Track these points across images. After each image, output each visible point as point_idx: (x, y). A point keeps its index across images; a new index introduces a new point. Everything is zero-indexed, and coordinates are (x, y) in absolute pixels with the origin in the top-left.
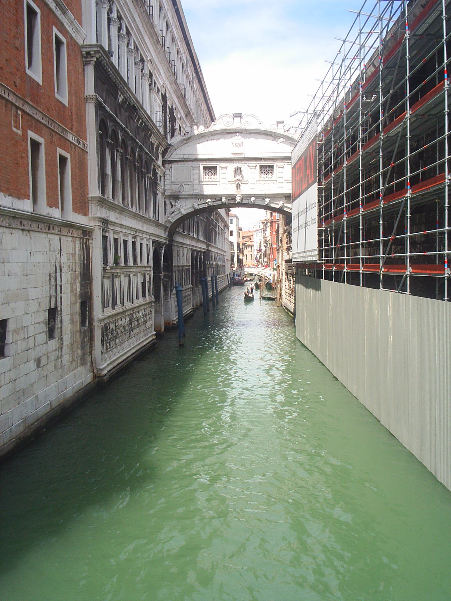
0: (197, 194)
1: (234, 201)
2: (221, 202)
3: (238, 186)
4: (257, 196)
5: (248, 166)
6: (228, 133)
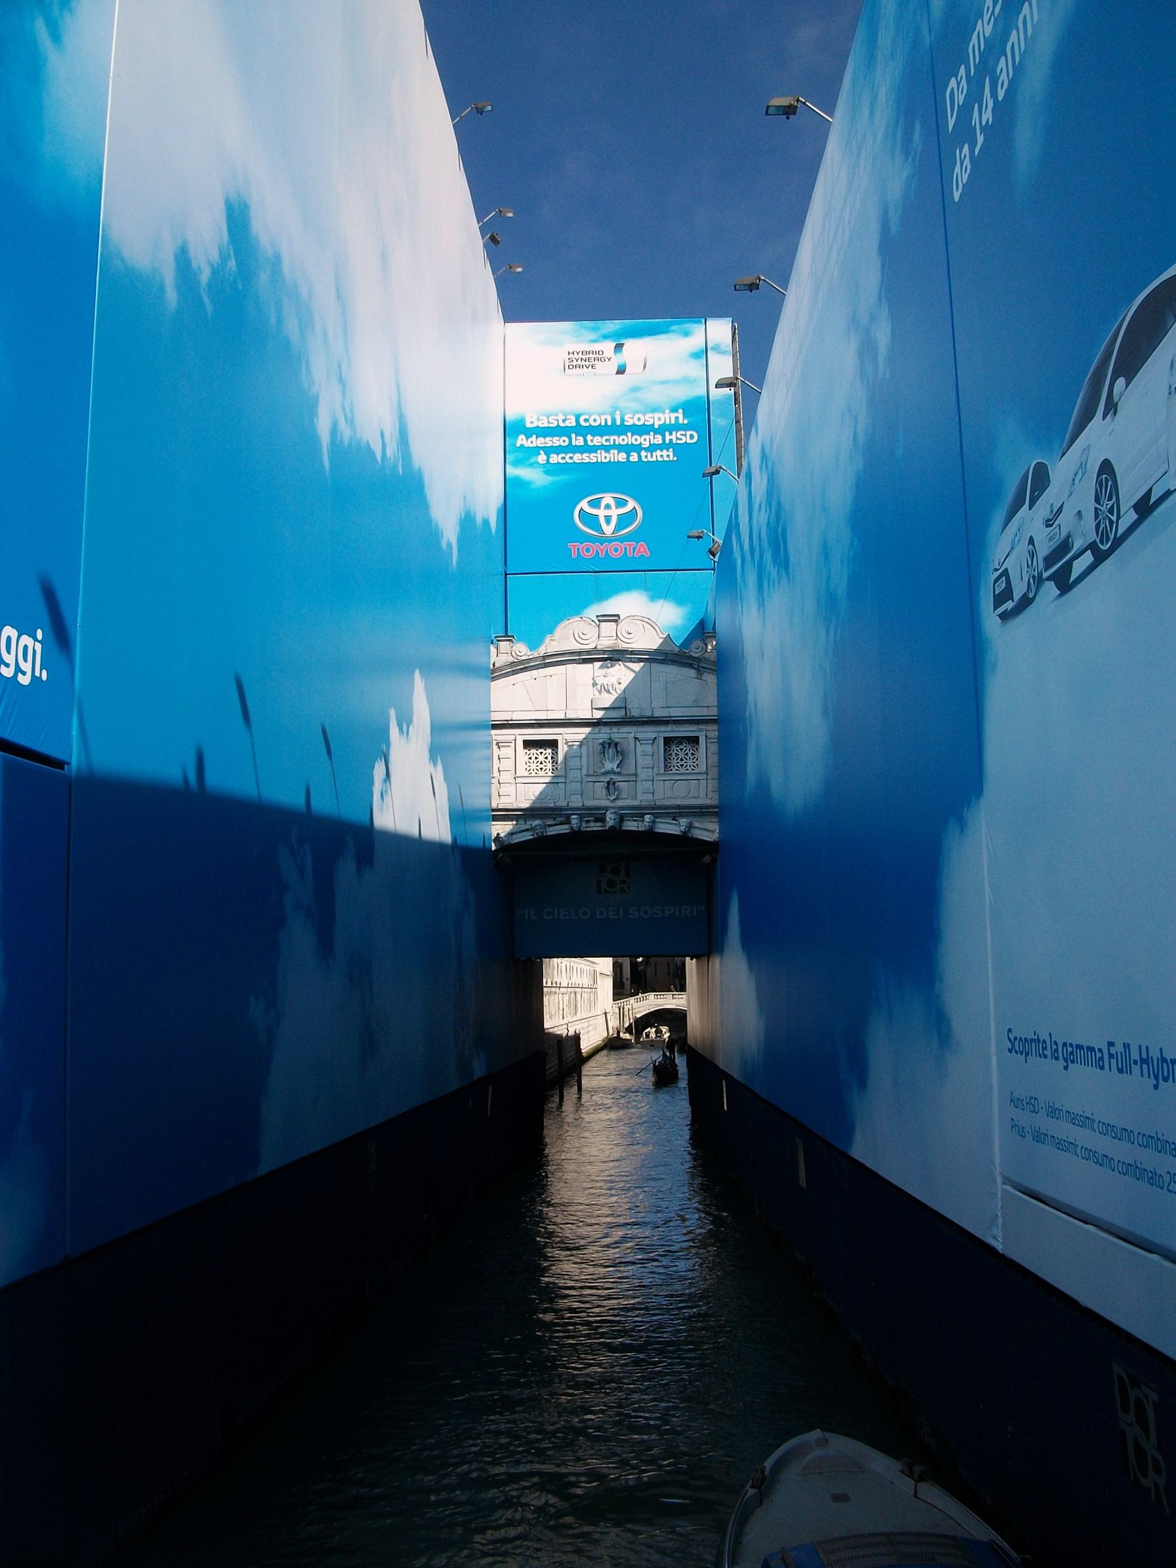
2: (567, 826)
3: (610, 785)
4: (660, 811)
5: (636, 738)
6: (585, 661)
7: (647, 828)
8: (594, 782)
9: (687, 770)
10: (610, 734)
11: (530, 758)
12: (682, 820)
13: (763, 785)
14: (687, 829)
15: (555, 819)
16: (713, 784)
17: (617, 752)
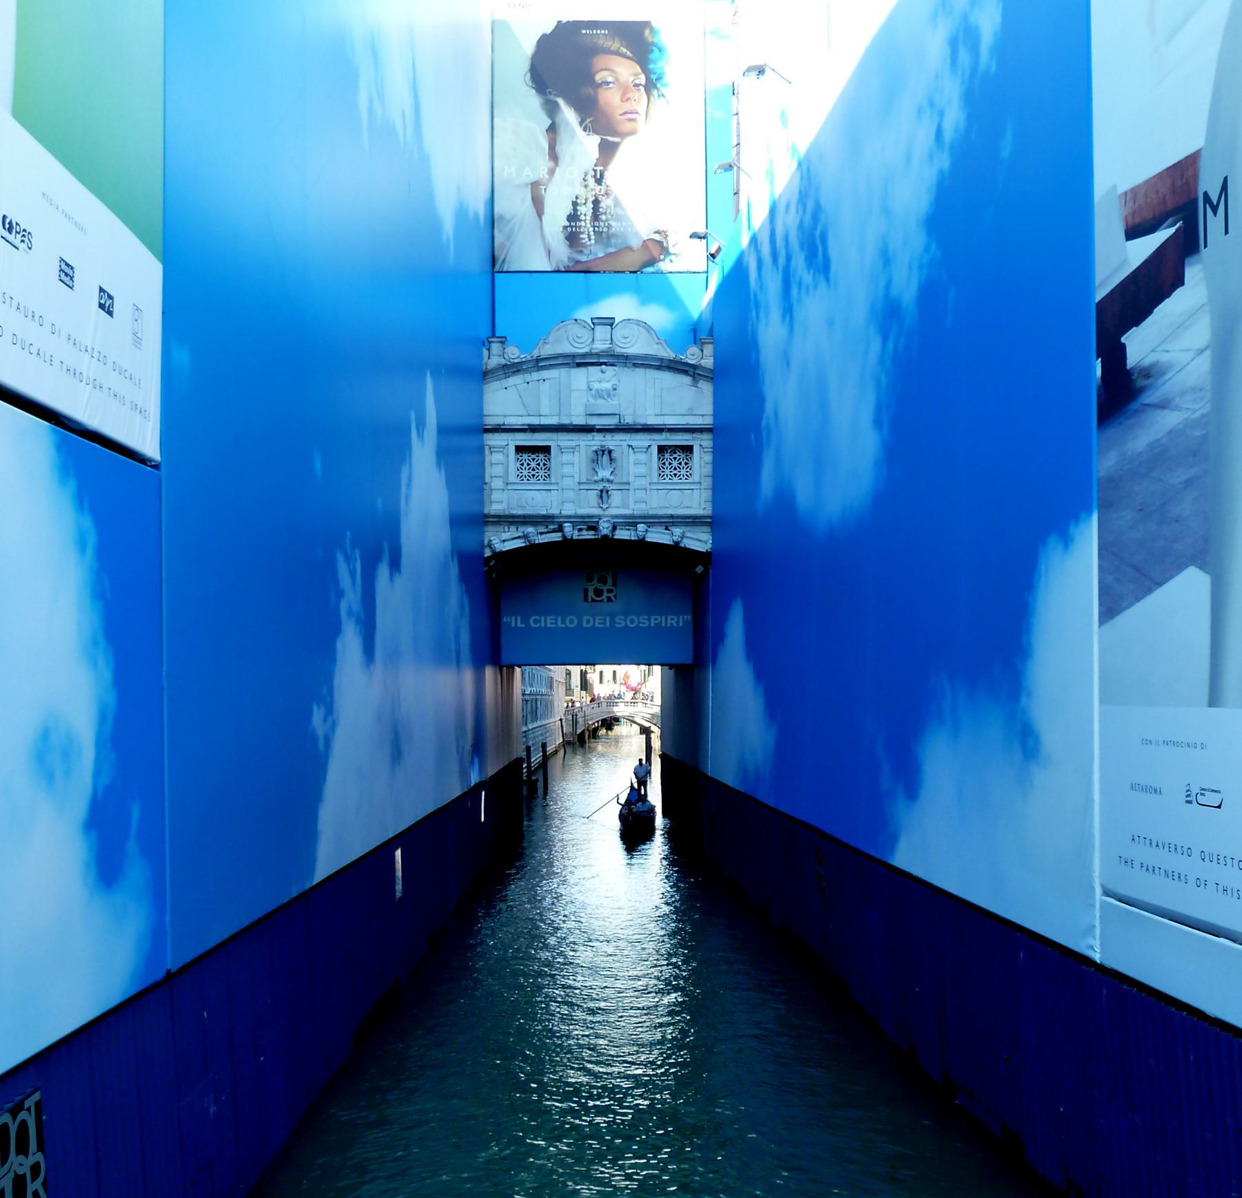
0: (501, 513)
1: (592, 532)
2: (559, 534)
3: (603, 494)
4: (652, 520)
5: (630, 446)
6: (579, 365)
7: (641, 537)
8: (587, 490)
9: (681, 479)
10: (602, 441)
11: (522, 465)
12: (675, 530)
13: (785, 499)
14: (679, 539)
15: (547, 528)
16: (707, 494)
17: (611, 460)
